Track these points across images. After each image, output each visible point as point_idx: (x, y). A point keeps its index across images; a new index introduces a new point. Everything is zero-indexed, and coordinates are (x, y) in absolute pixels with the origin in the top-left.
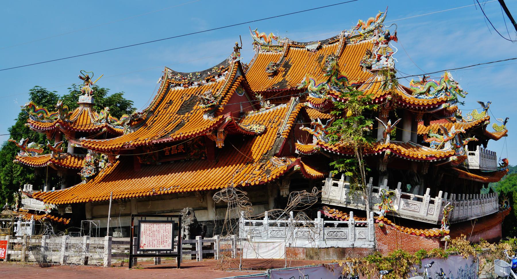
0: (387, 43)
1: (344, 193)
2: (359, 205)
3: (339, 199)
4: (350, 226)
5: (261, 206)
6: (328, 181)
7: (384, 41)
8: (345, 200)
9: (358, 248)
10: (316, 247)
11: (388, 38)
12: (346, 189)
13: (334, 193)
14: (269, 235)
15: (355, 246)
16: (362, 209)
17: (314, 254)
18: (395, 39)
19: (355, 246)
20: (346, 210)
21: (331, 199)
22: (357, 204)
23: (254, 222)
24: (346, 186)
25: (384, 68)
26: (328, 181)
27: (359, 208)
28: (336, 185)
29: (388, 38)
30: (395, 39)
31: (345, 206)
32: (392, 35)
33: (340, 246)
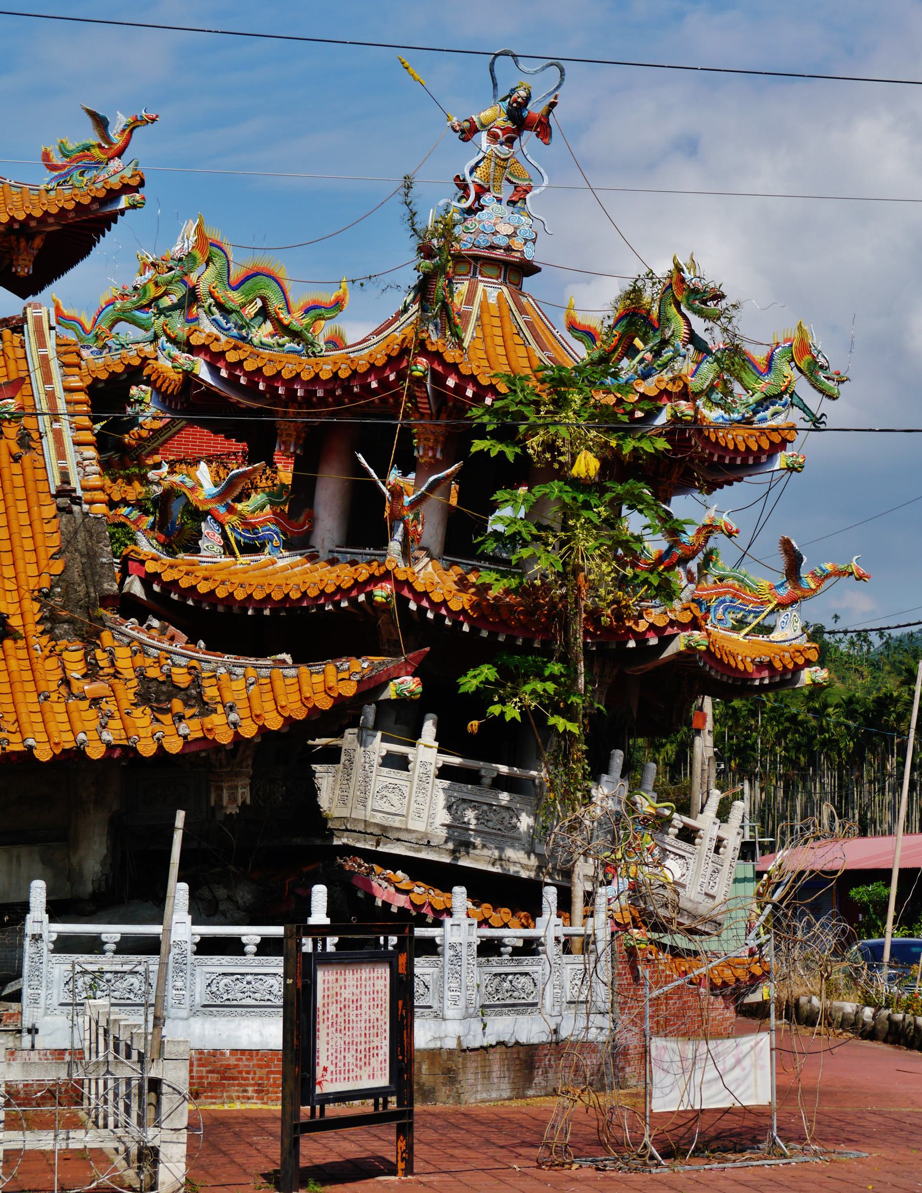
0: (510, 142)
1: (441, 800)
2: (510, 853)
3: (418, 825)
4: (551, 949)
5: (24, 851)
6: (362, 742)
7: (505, 130)
8: (443, 833)
9: (573, 1044)
10: (451, 1044)
11: (521, 120)
12: (446, 783)
13: (395, 798)
14: (200, 999)
15: (564, 1033)
16: (524, 874)
17: (440, 1079)
18: (543, 129)
19: (564, 1033)
20: (441, 876)
21: (384, 828)
22: (501, 849)
23: (112, 932)
24: (445, 772)
25: (493, 247)
26: (362, 742)
27: (512, 869)
28: (399, 763)
29: (521, 120)
30: (543, 129)
31: (447, 859)
32: (535, 108)
33: (523, 1040)
